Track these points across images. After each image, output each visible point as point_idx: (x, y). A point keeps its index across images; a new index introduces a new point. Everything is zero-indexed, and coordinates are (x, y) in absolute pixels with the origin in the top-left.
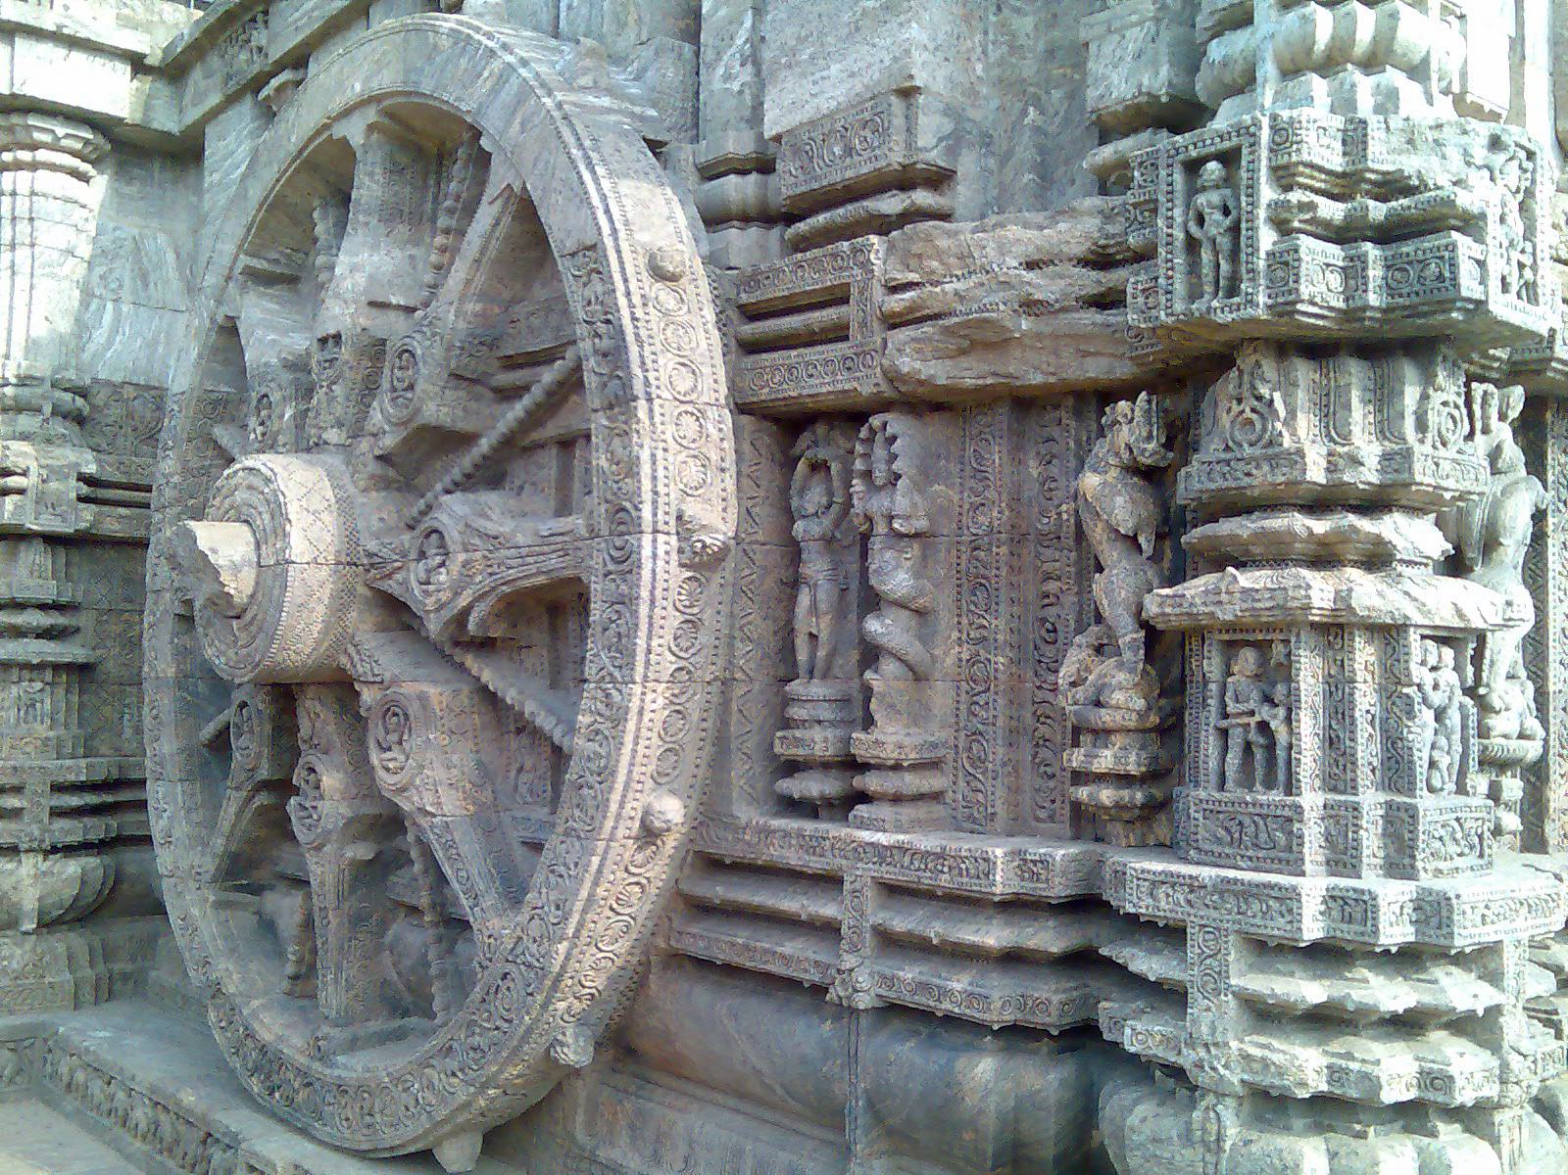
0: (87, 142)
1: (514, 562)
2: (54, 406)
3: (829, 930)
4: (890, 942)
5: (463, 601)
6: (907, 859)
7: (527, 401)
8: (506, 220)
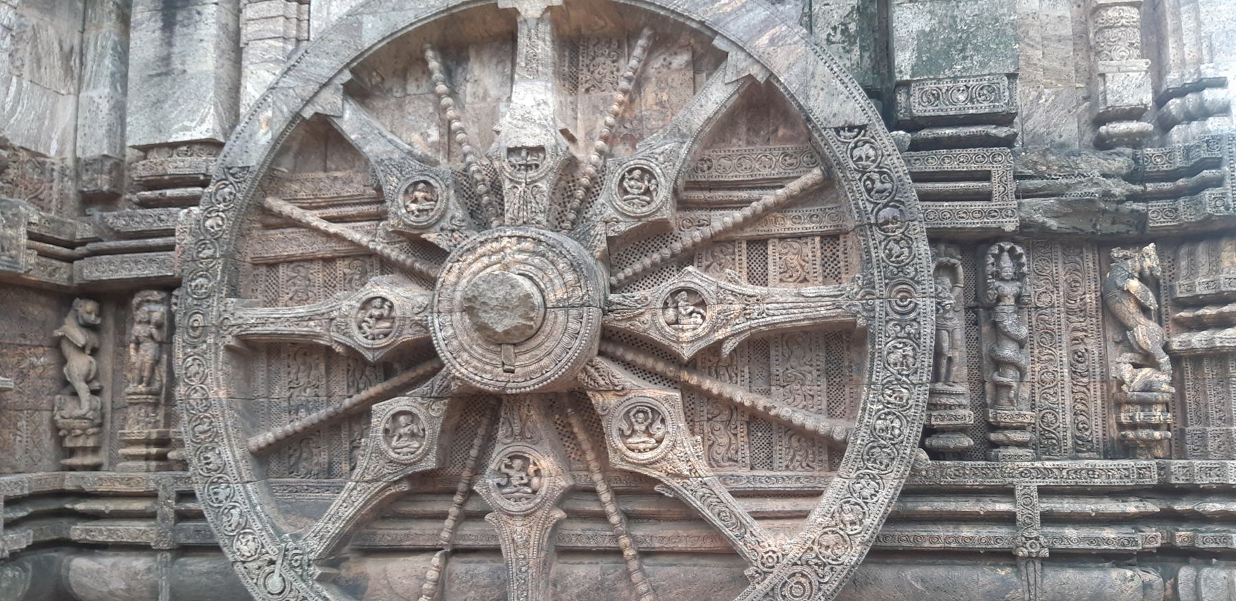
1: (776, 312)
3: (1008, 519)
4: (1049, 519)
5: (719, 335)
6: (1064, 473)
7: (747, 211)
8: (736, 96)
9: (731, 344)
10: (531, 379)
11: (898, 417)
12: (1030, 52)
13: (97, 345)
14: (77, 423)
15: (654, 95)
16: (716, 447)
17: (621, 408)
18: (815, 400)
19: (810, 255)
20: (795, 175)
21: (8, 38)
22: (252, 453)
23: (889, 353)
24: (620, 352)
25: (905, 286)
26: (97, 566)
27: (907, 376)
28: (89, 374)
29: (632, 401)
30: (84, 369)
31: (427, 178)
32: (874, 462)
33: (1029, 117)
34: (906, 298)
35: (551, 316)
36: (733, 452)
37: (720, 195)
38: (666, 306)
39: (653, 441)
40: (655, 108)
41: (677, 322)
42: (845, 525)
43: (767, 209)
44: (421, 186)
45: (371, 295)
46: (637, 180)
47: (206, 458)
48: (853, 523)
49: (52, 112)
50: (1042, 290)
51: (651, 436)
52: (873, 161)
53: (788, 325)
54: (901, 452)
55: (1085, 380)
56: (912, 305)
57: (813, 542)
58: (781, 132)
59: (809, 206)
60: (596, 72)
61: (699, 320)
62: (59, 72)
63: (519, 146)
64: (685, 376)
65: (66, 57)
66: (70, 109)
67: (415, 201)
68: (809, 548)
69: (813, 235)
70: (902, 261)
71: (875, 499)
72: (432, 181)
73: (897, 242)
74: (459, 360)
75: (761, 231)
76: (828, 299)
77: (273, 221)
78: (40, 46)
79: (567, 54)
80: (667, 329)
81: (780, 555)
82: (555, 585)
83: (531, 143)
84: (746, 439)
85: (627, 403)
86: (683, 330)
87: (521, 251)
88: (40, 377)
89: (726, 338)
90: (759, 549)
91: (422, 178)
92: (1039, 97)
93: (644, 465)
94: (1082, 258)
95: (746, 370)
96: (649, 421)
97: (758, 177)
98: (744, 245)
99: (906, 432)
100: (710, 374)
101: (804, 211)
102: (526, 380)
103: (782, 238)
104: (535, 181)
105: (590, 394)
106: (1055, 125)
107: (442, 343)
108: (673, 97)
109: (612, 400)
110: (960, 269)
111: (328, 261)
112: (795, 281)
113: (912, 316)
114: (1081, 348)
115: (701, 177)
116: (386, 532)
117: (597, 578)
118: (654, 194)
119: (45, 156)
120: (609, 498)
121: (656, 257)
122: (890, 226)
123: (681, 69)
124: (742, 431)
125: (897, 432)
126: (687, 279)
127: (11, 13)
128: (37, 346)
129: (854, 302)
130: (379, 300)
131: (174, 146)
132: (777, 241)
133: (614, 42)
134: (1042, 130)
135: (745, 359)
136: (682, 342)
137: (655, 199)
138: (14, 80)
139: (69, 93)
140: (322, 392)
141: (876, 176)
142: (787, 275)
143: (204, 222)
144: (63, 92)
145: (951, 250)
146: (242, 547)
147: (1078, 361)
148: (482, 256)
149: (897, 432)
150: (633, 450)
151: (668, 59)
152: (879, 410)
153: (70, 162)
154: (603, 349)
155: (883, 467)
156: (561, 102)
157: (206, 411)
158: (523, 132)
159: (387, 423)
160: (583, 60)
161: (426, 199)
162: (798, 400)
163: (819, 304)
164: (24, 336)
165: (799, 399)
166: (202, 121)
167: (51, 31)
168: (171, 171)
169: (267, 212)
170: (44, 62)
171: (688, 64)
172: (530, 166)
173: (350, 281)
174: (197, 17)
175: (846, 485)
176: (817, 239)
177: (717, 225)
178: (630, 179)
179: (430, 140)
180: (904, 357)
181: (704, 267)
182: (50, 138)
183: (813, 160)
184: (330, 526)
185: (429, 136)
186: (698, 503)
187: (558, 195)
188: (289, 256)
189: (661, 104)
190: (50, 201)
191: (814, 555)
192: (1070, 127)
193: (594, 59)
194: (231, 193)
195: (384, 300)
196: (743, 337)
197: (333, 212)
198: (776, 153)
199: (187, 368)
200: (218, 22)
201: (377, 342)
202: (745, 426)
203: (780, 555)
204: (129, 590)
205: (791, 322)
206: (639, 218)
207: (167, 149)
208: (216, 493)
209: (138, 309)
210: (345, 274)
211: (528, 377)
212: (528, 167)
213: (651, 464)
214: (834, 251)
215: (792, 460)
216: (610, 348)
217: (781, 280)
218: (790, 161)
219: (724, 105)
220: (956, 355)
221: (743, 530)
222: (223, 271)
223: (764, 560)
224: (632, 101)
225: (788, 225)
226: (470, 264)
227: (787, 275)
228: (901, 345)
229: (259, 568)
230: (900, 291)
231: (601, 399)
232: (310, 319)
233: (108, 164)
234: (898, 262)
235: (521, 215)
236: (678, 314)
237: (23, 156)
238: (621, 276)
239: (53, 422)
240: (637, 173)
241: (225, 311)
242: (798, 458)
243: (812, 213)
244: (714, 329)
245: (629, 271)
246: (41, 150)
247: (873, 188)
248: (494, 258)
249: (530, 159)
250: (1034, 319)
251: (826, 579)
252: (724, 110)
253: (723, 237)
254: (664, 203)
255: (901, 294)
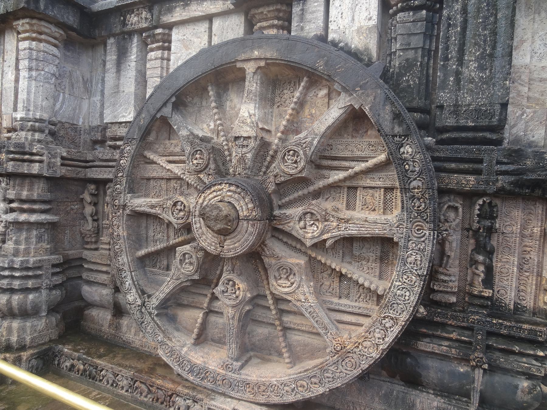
0: (61, 35)
2: (49, 131)
5: (325, 237)
8: (345, 115)
9: (330, 241)
10: (231, 252)
11: (409, 290)
12: (520, 88)
13: (96, 202)
14: (87, 232)
15: (308, 110)
16: (323, 286)
17: (276, 266)
18: (373, 270)
19: (378, 197)
20: (374, 156)
21: (54, 79)
22: (137, 258)
23: (408, 257)
24: (281, 237)
25: (420, 223)
26: (91, 290)
27: (416, 270)
28: (92, 214)
29: (281, 263)
30: (90, 212)
31: (201, 149)
32: (394, 310)
33: (514, 126)
34: (421, 230)
35: (240, 223)
36: (332, 289)
37: (336, 163)
38: (300, 219)
39: (289, 283)
40: (308, 117)
41: (305, 228)
42: (375, 339)
43: (356, 174)
44: (199, 152)
45: (177, 200)
46: (292, 156)
47: (118, 260)
48: (379, 338)
49: (80, 107)
50: (507, 223)
51: (289, 280)
52: (410, 155)
53: (359, 236)
54: (408, 308)
55: (527, 274)
56: (423, 234)
57: (359, 344)
58: (369, 133)
59: (379, 173)
60: (283, 97)
61: (315, 229)
62: (82, 89)
63: (240, 136)
64: (310, 252)
65: (85, 82)
66: (87, 106)
67: (196, 159)
68: (357, 346)
69: (380, 188)
70: (421, 210)
71: (392, 329)
72: (203, 150)
73: (419, 199)
74: (202, 239)
75: (354, 183)
76: (380, 225)
77: (148, 161)
78: (73, 79)
79: (270, 88)
80: (300, 231)
81: (343, 346)
82: (249, 334)
83: (245, 135)
84: (338, 284)
85: (279, 264)
86: (307, 233)
87: (229, 191)
88: (75, 213)
89: (328, 238)
90: (334, 342)
91: (199, 149)
92: (522, 115)
93: (285, 294)
94: (535, 208)
95: (341, 252)
96: (288, 274)
97: (355, 156)
98: (346, 190)
99: (412, 299)
100: (323, 251)
101: (376, 175)
102: (228, 252)
103: (364, 188)
104: (246, 153)
105: (263, 257)
106: (531, 130)
107: (195, 230)
108: (317, 112)
109: (273, 261)
110: (460, 210)
111: (169, 180)
112: (369, 210)
113: (423, 239)
114: (528, 257)
115: (327, 154)
116: (185, 298)
117: (266, 335)
118: (299, 163)
119: (77, 125)
120: (272, 303)
121: (300, 193)
122: (416, 190)
123: (322, 98)
124: (337, 280)
125: (407, 298)
126: (311, 207)
127: (55, 68)
128: (73, 202)
129: (393, 228)
130: (180, 202)
131: (121, 123)
132: (362, 189)
133: (292, 82)
134: (522, 133)
135: (341, 247)
136: (307, 238)
137: (299, 166)
138: (62, 94)
139: (87, 99)
140: (165, 235)
141: (411, 163)
142: (366, 207)
143: (120, 161)
144: (85, 98)
145: (457, 199)
146: (129, 298)
147: (524, 263)
148: (214, 191)
149: (407, 298)
150: (280, 286)
151: (317, 92)
152: (399, 286)
153: (87, 127)
154: (273, 235)
155: (398, 314)
156: (265, 112)
157: (119, 240)
158: (242, 129)
159: (181, 256)
160: (278, 92)
161: (200, 158)
162: (365, 270)
163: (376, 227)
164: (68, 198)
165: (365, 268)
166: (130, 113)
167: (78, 72)
168: (119, 134)
169: (145, 157)
170: (75, 86)
171: (325, 96)
172: (245, 145)
173: (176, 189)
174: (128, 68)
175: (378, 320)
176: (382, 190)
177: (331, 180)
178: (288, 155)
179: (211, 128)
180: (416, 260)
181: (325, 199)
182: (79, 118)
183: (384, 149)
184: (161, 295)
185: (210, 126)
186: (308, 315)
187: (259, 158)
188: (153, 177)
189: (311, 115)
190: (80, 143)
191: (359, 350)
192: (540, 132)
193: (283, 91)
194: (129, 149)
195: (182, 203)
196: (336, 239)
197: (171, 158)
198: (365, 143)
199: (113, 222)
200: (136, 69)
201: (179, 221)
202: (338, 278)
203: (343, 346)
204: (101, 301)
205: (361, 234)
206: (291, 175)
207: (118, 124)
208: (121, 274)
209: (108, 189)
210: (174, 186)
211: (229, 250)
212: (243, 146)
213: (287, 294)
214: (391, 196)
215: (359, 298)
216: (277, 235)
217: (362, 209)
218: (371, 148)
219: (337, 119)
220: (452, 254)
221: (327, 331)
222: (126, 183)
223: (335, 347)
224: (298, 113)
225: (368, 182)
226: (208, 195)
227: (366, 207)
228: (415, 254)
229: (135, 307)
230: (417, 226)
231: (268, 261)
232: (156, 207)
233: (100, 129)
234: (418, 210)
235: (237, 170)
236: (305, 225)
237: (67, 125)
238: (283, 201)
239: (80, 231)
240: (291, 152)
241: (127, 199)
242: (362, 297)
243: (381, 176)
244: (322, 233)
245: (287, 199)
246: (75, 123)
247: (409, 169)
248: (218, 193)
249: (245, 143)
250: (500, 239)
251: (364, 362)
252: (338, 122)
253: (335, 185)
254: (303, 169)
255: (418, 227)
